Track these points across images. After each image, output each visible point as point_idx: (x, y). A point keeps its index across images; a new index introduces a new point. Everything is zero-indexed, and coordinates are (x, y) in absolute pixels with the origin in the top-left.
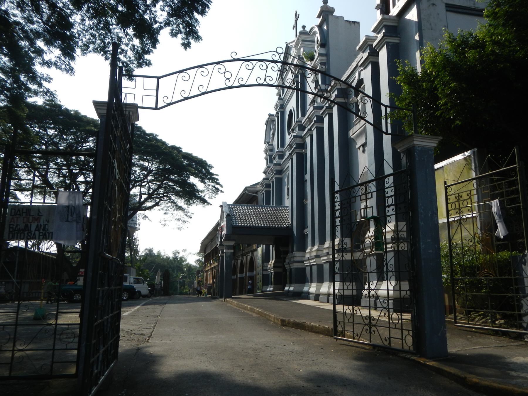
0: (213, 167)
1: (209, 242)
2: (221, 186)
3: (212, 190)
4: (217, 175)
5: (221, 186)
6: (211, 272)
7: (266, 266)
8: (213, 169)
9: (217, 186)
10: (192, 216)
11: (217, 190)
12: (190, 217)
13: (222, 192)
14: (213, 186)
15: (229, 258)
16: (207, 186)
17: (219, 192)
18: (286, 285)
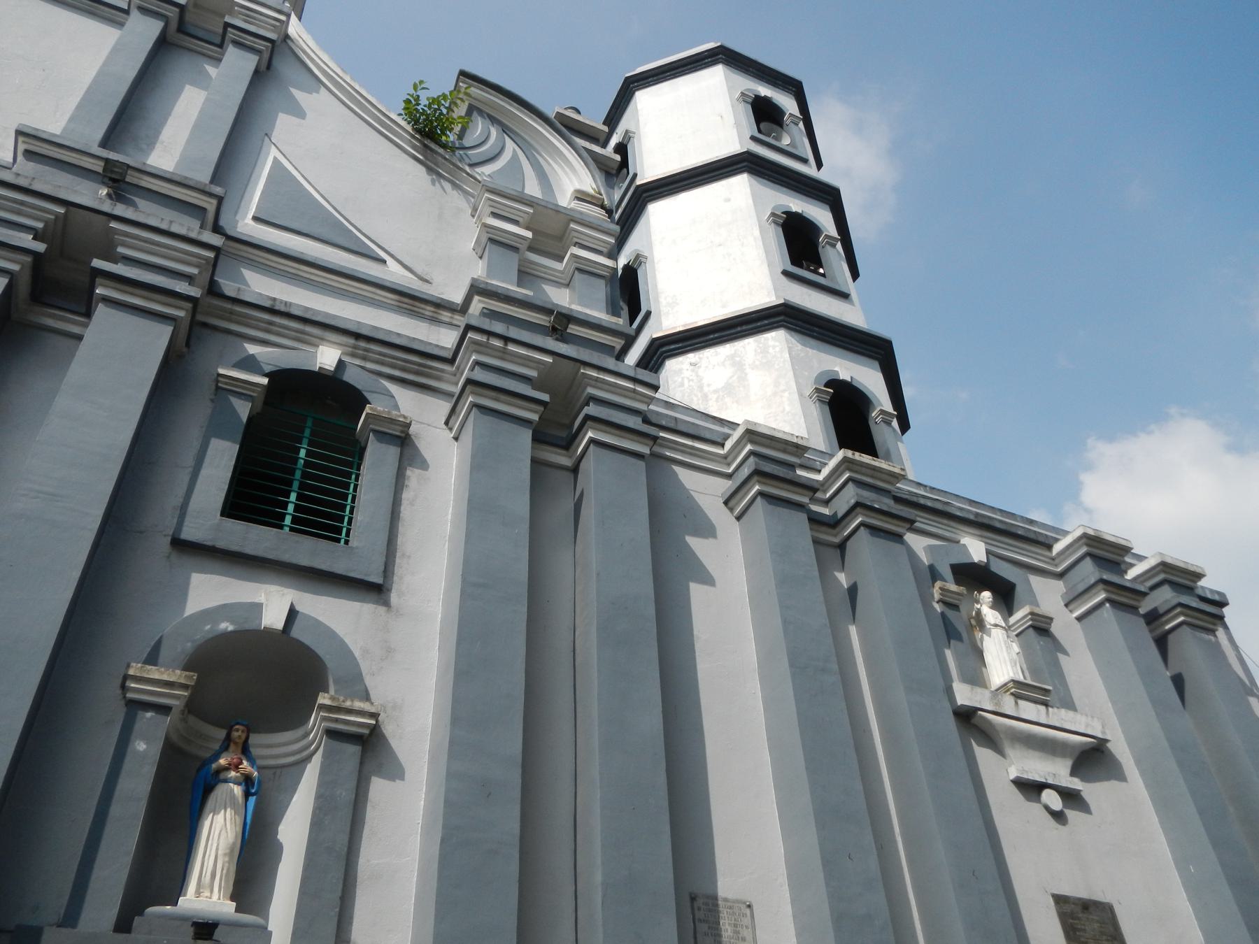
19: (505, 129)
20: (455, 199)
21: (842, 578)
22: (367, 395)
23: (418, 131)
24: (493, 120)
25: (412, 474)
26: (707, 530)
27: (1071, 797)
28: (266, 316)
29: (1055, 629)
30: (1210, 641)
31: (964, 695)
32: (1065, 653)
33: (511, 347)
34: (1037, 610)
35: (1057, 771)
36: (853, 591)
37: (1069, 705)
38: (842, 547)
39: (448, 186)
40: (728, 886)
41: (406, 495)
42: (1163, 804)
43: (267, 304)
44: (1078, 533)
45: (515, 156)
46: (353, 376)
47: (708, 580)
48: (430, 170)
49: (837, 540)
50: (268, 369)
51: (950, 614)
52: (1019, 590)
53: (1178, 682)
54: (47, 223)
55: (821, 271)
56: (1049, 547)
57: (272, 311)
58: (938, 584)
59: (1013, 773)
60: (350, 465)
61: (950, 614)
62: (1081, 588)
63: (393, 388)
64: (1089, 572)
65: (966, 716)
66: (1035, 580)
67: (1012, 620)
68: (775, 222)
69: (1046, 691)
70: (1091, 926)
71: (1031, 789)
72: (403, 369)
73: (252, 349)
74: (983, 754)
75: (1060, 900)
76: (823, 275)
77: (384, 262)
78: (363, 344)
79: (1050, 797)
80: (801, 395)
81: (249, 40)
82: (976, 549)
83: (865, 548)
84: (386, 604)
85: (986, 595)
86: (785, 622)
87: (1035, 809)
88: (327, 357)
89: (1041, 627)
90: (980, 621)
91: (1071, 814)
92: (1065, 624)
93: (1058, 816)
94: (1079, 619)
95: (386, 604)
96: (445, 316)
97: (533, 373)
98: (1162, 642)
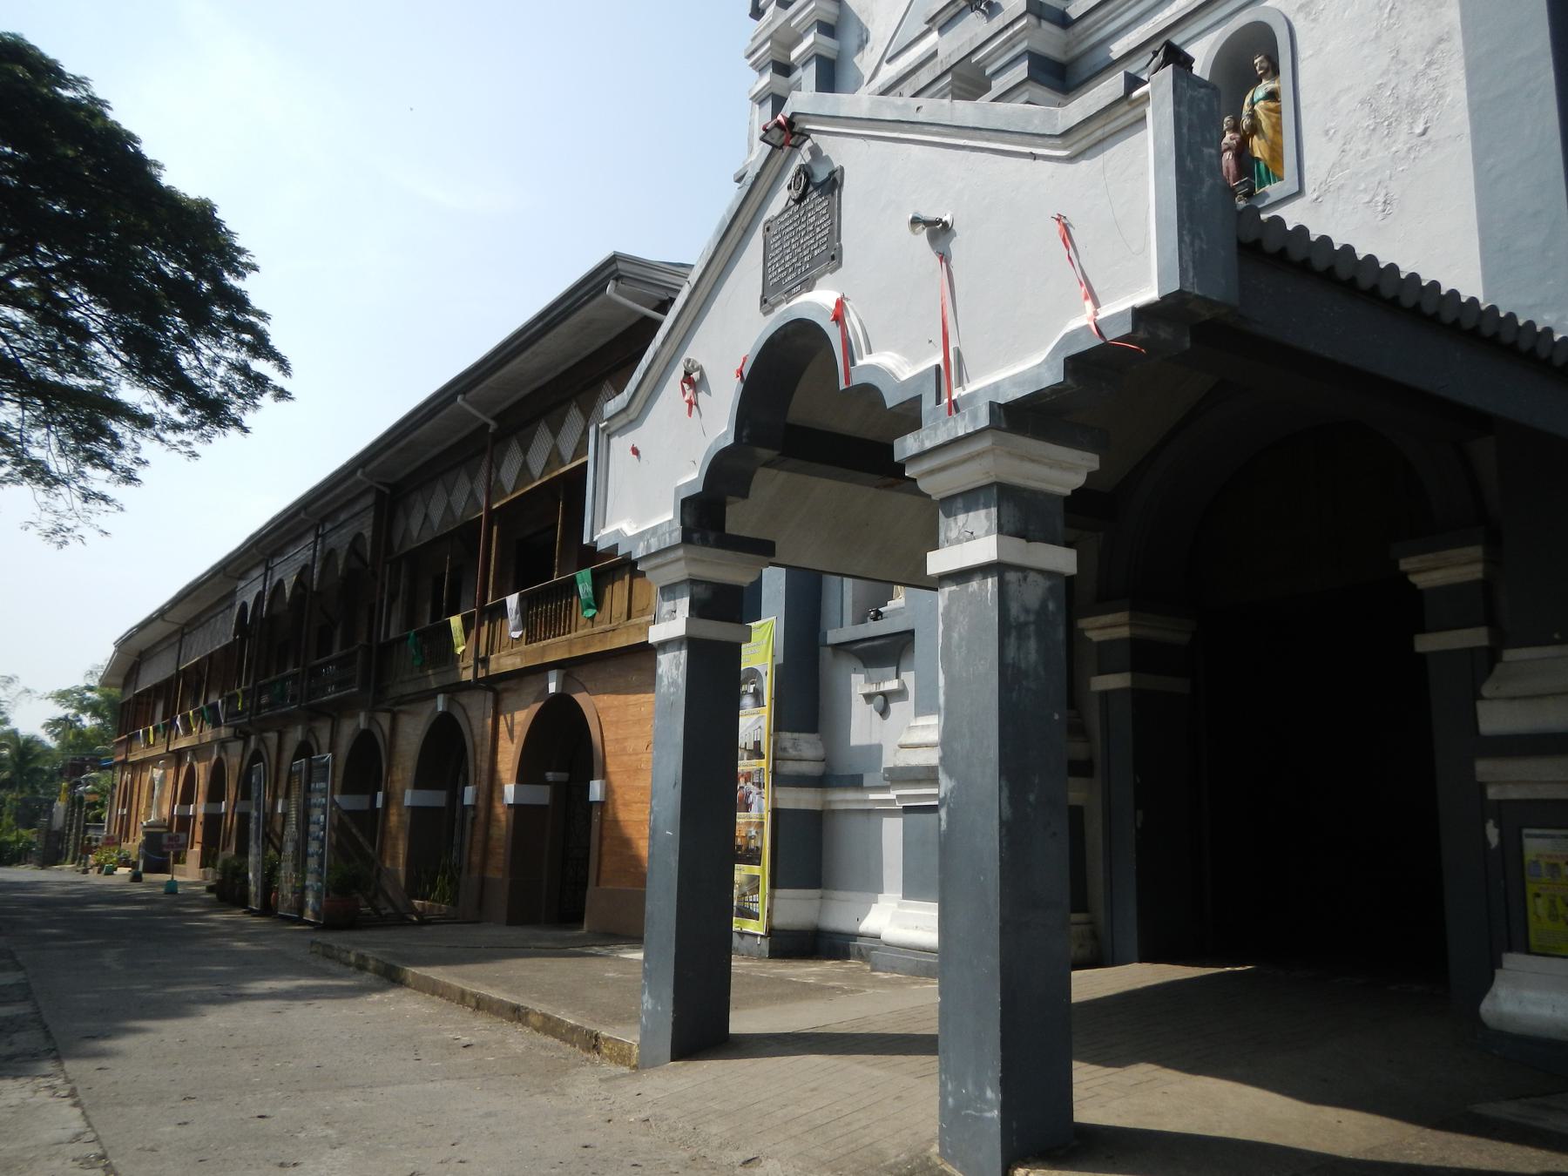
0: (255, 268)
1: (175, 632)
2: (283, 364)
3: (227, 384)
4: (262, 315)
5: (281, 368)
6: (171, 772)
7: (792, 753)
8: (252, 276)
9: (260, 366)
10: (140, 473)
11: (260, 382)
12: (129, 478)
13: (281, 394)
14: (233, 366)
15: (1032, 644)
16: (205, 364)
17: (266, 400)
18: (1498, 964)
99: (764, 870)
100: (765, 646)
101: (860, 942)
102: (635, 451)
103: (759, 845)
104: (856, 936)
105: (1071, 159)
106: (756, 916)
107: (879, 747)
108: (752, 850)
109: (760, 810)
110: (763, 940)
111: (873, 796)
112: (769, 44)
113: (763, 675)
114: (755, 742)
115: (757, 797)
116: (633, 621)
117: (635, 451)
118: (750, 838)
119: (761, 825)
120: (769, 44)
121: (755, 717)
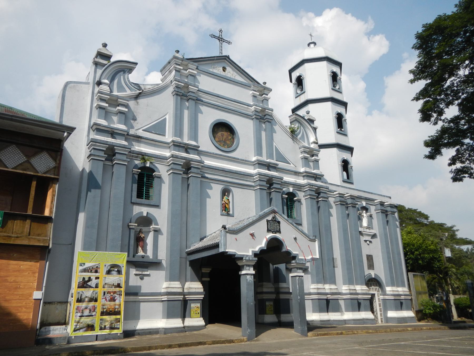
19: (301, 124)
20: (297, 147)
21: (347, 212)
22: (296, 195)
23: (291, 132)
24: (299, 122)
25: (301, 206)
26: (332, 208)
27: (370, 242)
28: (284, 184)
29: (373, 216)
30: (393, 216)
31: (360, 229)
32: (373, 219)
33: (313, 187)
34: (371, 214)
35: (369, 238)
36: (348, 215)
37: (372, 229)
38: (347, 207)
39: (295, 143)
40: (335, 257)
41: (301, 210)
42: (381, 242)
43: (284, 182)
44: (379, 201)
45: (303, 132)
46: (294, 192)
47: (332, 216)
48: (293, 139)
49: (347, 206)
50: (286, 193)
51: (360, 216)
52: (369, 210)
53: (387, 221)
54: (267, 180)
55: (343, 130)
56: (374, 201)
57: (285, 183)
58: (359, 212)
59: (364, 239)
60: (293, 204)
61: (360, 216)
62: (377, 209)
63: (297, 192)
64: (379, 207)
65: (360, 232)
66: (371, 206)
67: (367, 214)
68: (336, 118)
69: (370, 227)
70: (370, 258)
71: (366, 241)
72: (298, 188)
73: (284, 189)
74: (361, 237)
75: (367, 255)
76: (343, 131)
77: (290, 164)
78: (294, 186)
79: (368, 242)
80: (338, 164)
81: (270, 120)
82: (364, 204)
83: (351, 209)
84: (302, 226)
85: (364, 211)
86: (342, 224)
87: (366, 243)
88: (291, 190)
89: (371, 216)
90: (363, 216)
91: (370, 244)
92: (374, 216)
93: (368, 244)
94: (376, 213)
95: (302, 226)
96: (300, 174)
97: (315, 190)
98: (387, 215)
99: (121, 317)
100: (122, 259)
101: (136, 332)
102: (236, 240)
103: (120, 310)
104: (136, 330)
105: (309, 241)
106: (118, 329)
107: (140, 287)
108: (116, 312)
109: (120, 301)
110: (121, 334)
111: (140, 298)
112: (109, 97)
113: (122, 267)
114: (118, 284)
115: (119, 298)
116: (30, 236)
117: (236, 240)
118: (116, 308)
119: (120, 305)
120: (109, 97)
121: (119, 277)
